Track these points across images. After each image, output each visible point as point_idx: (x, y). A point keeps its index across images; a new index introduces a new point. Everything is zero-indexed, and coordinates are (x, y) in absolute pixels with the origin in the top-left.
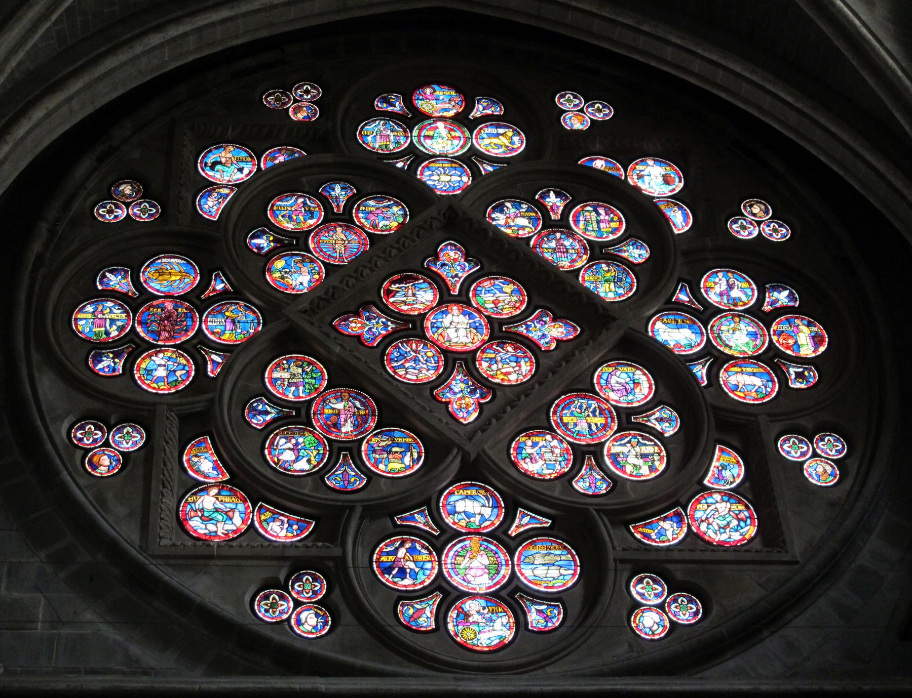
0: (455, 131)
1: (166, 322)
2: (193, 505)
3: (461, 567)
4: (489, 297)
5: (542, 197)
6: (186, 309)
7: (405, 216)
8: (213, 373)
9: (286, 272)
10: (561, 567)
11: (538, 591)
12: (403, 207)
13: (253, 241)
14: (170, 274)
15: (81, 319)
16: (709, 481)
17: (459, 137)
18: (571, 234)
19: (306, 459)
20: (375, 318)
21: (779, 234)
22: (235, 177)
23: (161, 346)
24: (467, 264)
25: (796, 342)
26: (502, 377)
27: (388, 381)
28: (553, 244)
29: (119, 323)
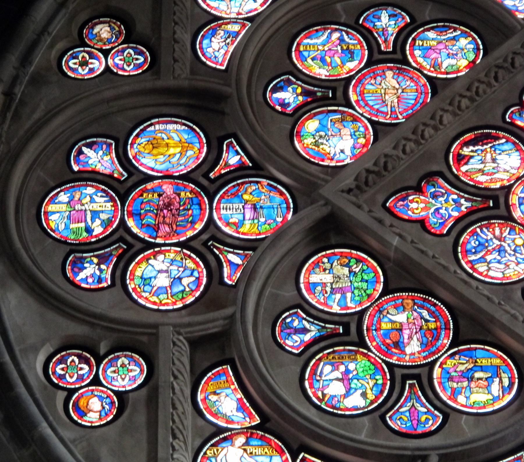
8: (230, 280)
9: (321, 137)
12: (474, 38)
13: (275, 95)
14: (167, 145)
15: (54, 213)
19: (359, 392)
20: (443, 195)
27: (466, 282)
29: (104, 216)
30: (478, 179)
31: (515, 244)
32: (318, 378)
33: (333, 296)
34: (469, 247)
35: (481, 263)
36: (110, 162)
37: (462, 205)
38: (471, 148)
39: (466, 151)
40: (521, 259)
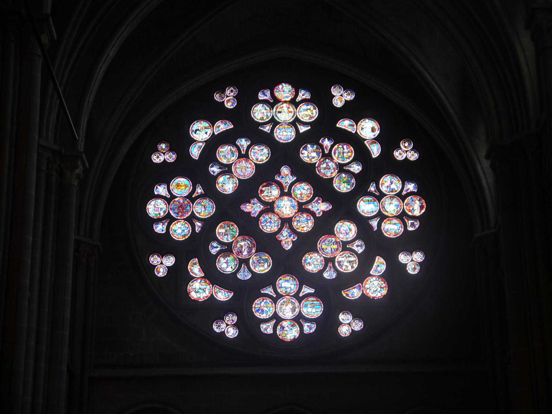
0: (290, 108)
1: (180, 208)
2: (192, 286)
3: (283, 309)
5: (322, 142)
6: (187, 202)
7: (269, 154)
8: (197, 231)
9: (224, 184)
11: (308, 318)
12: (268, 149)
14: (181, 186)
15: (150, 208)
16: (372, 272)
18: (332, 159)
19: (230, 266)
21: (413, 156)
23: (179, 219)
24: (291, 177)
26: (301, 229)
28: (325, 165)
29: (164, 210)
34: (262, 221)
38: (265, 188)
39: (263, 189)
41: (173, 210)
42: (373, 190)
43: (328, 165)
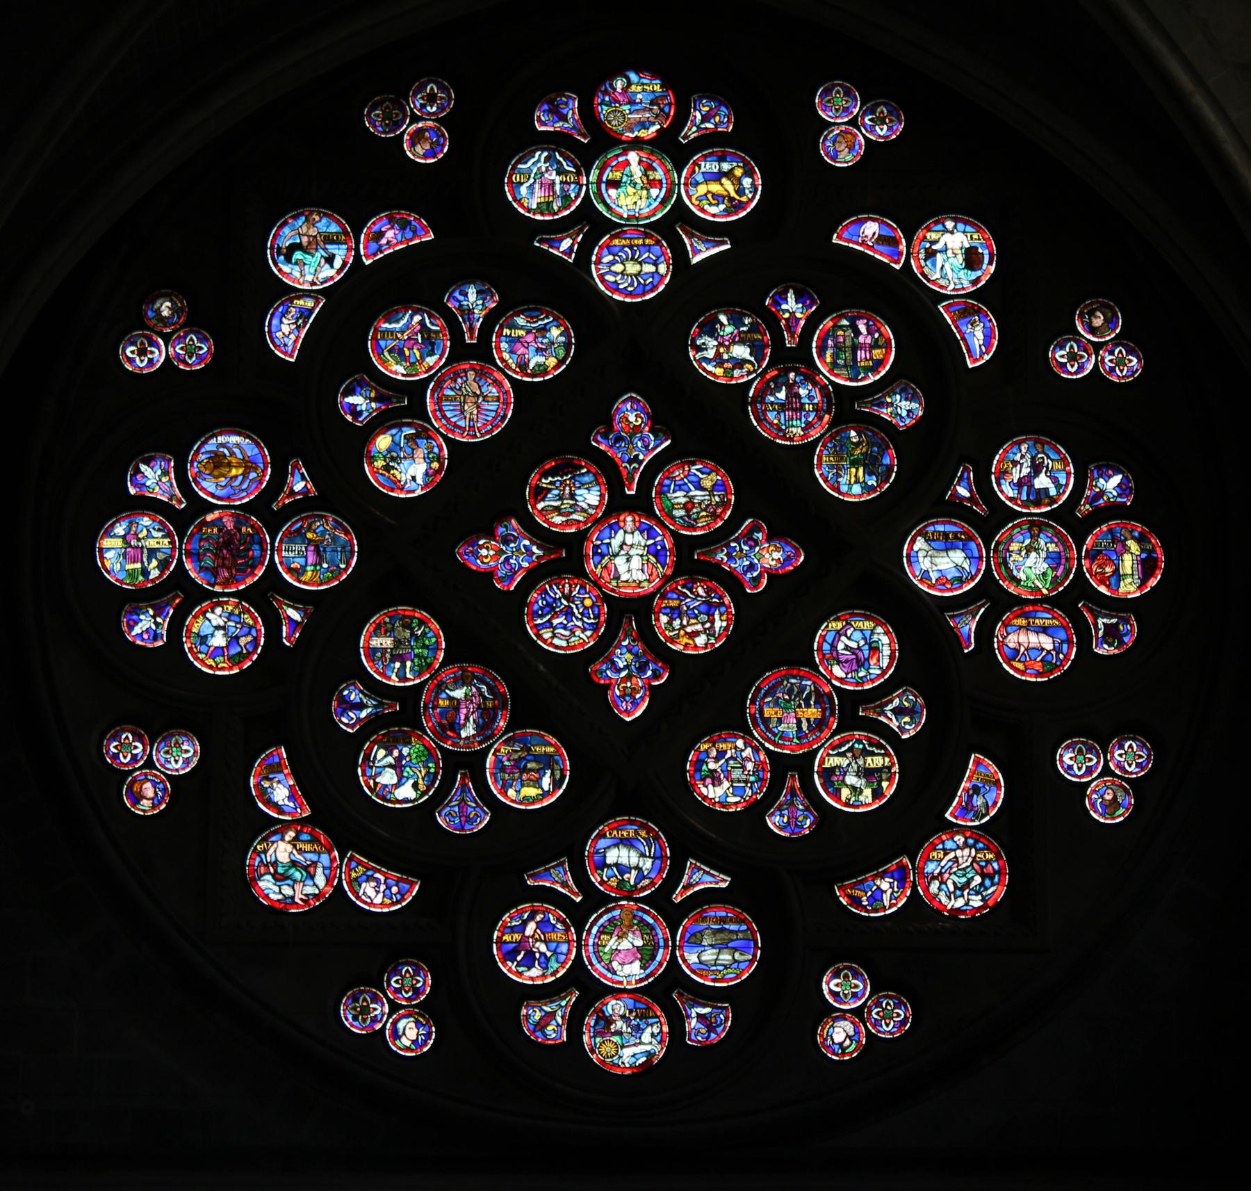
0: (654, 169)
1: (225, 551)
3: (607, 949)
4: (679, 497)
5: (776, 303)
6: (252, 527)
7: (567, 346)
8: (289, 641)
9: (393, 459)
10: (735, 949)
12: (567, 329)
15: (109, 549)
16: (952, 814)
17: (660, 181)
18: (811, 374)
19: (411, 782)
22: (322, 276)
25: (1116, 571)
26: (685, 640)
29: (160, 556)
30: (553, 520)
31: (584, 606)
32: (371, 764)
33: (392, 665)
34: (536, 607)
35: (546, 628)
36: (168, 484)
37: (534, 553)
39: (545, 482)
40: (587, 623)
41: (195, 558)
42: (968, 495)
43: (798, 396)
